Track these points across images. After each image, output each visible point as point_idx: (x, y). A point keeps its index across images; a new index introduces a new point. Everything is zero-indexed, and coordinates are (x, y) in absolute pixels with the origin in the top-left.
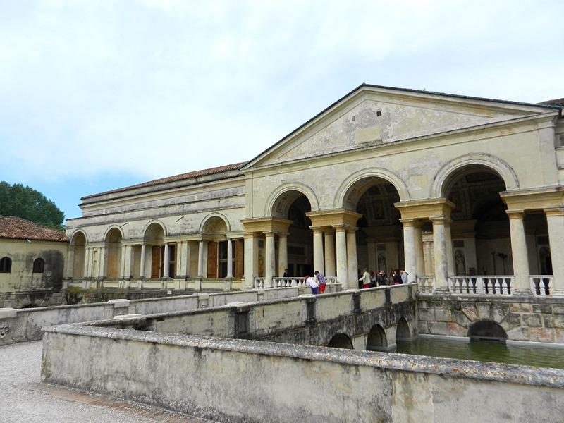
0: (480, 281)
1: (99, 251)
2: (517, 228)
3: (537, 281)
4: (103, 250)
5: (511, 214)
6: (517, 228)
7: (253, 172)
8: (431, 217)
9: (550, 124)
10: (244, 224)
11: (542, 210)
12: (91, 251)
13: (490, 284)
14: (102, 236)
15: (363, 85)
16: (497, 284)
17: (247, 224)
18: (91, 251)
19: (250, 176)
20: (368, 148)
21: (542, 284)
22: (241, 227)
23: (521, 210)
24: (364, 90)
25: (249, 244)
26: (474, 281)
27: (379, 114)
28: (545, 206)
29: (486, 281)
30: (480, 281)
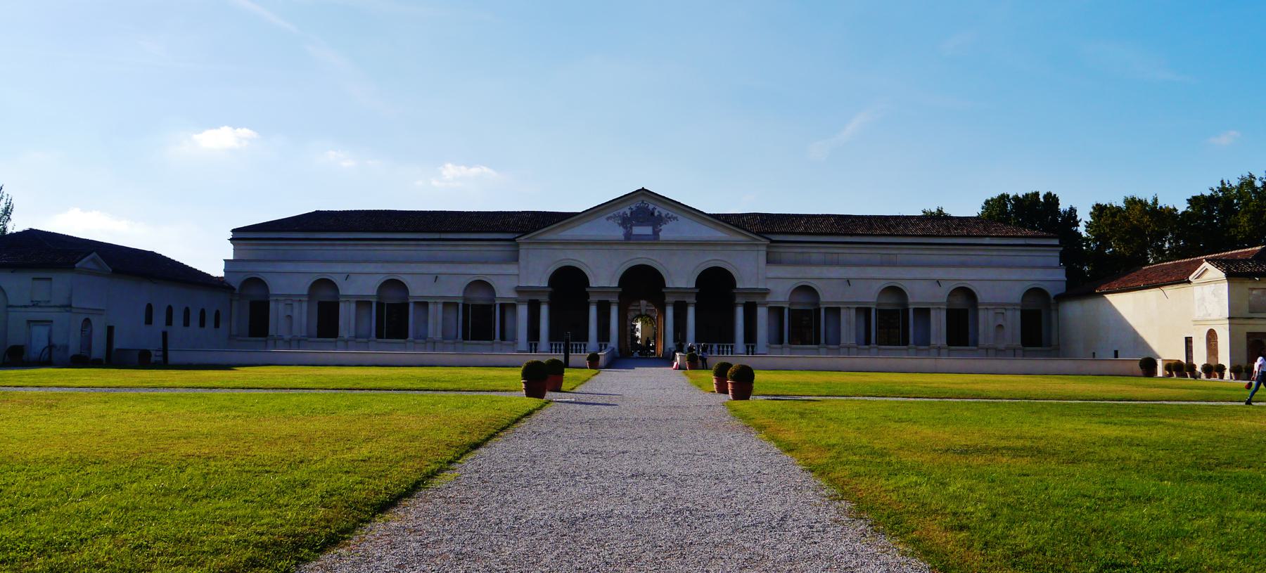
0: (715, 346)
1: (296, 305)
2: (740, 312)
3: (748, 347)
4: (305, 305)
6: (740, 312)
7: (529, 243)
8: (688, 300)
9: (764, 248)
11: (755, 302)
12: (281, 306)
13: (721, 349)
14: (302, 286)
16: (725, 349)
17: (520, 290)
18: (281, 306)
19: (525, 247)
20: (641, 241)
22: (513, 295)
23: (744, 302)
25: (523, 311)
26: (711, 347)
27: (652, 214)
28: (758, 300)
29: (719, 347)
30: (715, 346)
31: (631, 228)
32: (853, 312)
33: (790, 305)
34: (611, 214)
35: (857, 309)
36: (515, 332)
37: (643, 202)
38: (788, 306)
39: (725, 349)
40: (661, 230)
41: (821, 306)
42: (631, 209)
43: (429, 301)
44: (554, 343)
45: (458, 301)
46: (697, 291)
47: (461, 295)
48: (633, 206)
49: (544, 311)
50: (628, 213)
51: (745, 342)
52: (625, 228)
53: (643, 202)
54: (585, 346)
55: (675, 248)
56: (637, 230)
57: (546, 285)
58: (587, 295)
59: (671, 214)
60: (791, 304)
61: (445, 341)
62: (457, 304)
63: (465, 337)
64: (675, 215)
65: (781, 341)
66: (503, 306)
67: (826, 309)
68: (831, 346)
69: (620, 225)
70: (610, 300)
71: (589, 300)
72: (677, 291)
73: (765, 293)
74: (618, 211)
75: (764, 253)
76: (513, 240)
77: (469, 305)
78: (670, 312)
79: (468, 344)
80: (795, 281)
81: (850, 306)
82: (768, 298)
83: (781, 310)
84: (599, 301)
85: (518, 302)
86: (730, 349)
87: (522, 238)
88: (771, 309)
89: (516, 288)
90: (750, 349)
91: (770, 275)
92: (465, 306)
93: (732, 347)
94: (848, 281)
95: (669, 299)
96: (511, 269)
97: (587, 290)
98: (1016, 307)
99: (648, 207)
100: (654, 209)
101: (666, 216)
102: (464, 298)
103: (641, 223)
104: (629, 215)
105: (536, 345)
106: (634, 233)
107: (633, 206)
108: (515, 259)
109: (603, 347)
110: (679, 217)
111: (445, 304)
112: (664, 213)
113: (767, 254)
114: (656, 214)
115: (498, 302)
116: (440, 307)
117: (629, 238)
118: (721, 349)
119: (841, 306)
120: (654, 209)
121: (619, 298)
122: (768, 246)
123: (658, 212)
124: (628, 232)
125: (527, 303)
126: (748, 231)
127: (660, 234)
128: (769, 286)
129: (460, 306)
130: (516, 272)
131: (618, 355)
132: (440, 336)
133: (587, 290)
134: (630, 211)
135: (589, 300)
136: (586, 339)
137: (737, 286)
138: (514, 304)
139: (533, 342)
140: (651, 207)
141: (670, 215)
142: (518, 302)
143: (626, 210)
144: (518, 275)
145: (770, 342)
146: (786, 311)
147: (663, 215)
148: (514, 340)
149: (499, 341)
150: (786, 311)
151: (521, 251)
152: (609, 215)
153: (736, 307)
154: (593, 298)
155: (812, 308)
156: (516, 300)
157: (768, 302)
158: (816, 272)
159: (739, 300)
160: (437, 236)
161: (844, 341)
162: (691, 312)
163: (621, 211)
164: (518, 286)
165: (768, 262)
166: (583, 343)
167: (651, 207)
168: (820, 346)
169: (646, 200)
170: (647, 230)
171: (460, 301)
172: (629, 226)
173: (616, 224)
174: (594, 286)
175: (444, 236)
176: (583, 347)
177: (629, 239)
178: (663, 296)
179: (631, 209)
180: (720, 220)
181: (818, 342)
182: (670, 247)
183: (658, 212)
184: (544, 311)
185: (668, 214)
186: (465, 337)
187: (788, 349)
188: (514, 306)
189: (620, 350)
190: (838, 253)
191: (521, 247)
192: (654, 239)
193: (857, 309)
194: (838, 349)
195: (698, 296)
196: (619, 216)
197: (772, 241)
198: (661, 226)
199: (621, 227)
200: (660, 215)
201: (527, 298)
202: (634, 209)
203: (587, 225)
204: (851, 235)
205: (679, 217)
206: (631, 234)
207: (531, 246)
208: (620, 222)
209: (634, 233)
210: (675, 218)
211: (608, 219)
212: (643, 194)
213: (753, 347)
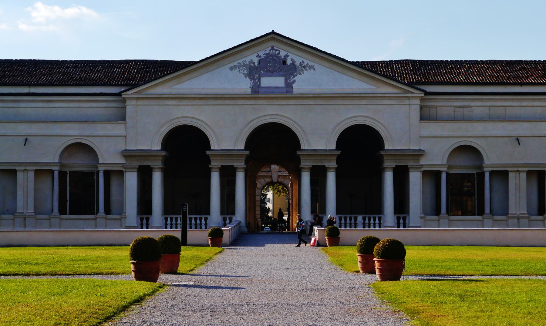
0: (360, 218)
2: (389, 178)
3: (398, 219)
5: (386, 168)
6: (389, 178)
7: (138, 98)
8: (327, 165)
9: (418, 102)
10: (124, 155)
13: (367, 221)
15: (273, 32)
16: (372, 221)
17: (128, 155)
19: (134, 102)
21: (401, 221)
22: (122, 161)
23: (394, 165)
24: (273, 37)
26: (356, 219)
27: (284, 62)
28: (410, 164)
29: (364, 219)
31: (259, 79)
32: (524, 176)
33: (448, 168)
34: (236, 63)
35: (529, 173)
36: (122, 204)
37: (273, 48)
38: (445, 169)
39: (372, 221)
40: (294, 81)
41: (485, 169)
42: (258, 56)
43: (17, 168)
44: (169, 217)
45: (53, 168)
46: (339, 153)
47: (57, 160)
48: (262, 54)
49: (157, 178)
50: (256, 61)
51: (395, 213)
52: (252, 79)
53: (273, 48)
54: (206, 219)
55: (311, 102)
56: (266, 82)
57: (159, 148)
58: (208, 160)
59: (306, 62)
60: (449, 167)
61: (38, 216)
62: (52, 172)
63: (62, 211)
64: (311, 64)
65: (437, 211)
66: (107, 174)
67: (492, 173)
68: (496, 217)
69: (246, 76)
70: (236, 164)
71: (210, 166)
72: (315, 153)
73: (418, 154)
74: (244, 59)
75: (418, 108)
76: (119, 94)
77: (65, 173)
78: (306, 178)
79: (67, 219)
80: (456, 140)
81: (520, 169)
82: (423, 161)
83: (438, 174)
84: (222, 166)
86: (377, 221)
87: (130, 92)
88: (425, 173)
89: (123, 152)
90: (401, 221)
91: (425, 133)
92: (62, 174)
93: (380, 219)
94: (517, 139)
95: (306, 163)
96: (118, 129)
97: (208, 153)
99: (279, 54)
100: (287, 56)
101: (301, 64)
102: (61, 165)
103: (271, 74)
104: (256, 64)
105: (148, 219)
106: (262, 85)
107: (262, 54)
108: (122, 118)
109: (228, 221)
110: (316, 66)
111: (38, 173)
113: (421, 108)
114: (289, 62)
115: (101, 169)
116: (31, 175)
117: (256, 90)
118: (367, 221)
119: (509, 169)
120: (287, 56)
121: (246, 162)
122: (422, 99)
123: (292, 60)
124: (255, 84)
125: (136, 170)
126: (398, 81)
127: (294, 85)
128: (423, 146)
129: (56, 174)
131: (245, 229)
132: (31, 210)
133: (208, 153)
134: (258, 58)
135: (210, 166)
136: (207, 211)
137: (387, 147)
138: (122, 170)
139: (145, 216)
140: (282, 54)
141: (305, 64)
142: (126, 168)
143: (253, 57)
145: (425, 212)
146: (444, 176)
147: (297, 64)
148: (121, 213)
149: (104, 215)
150: (444, 176)
151: (128, 107)
152: (232, 65)
153: (384, 172)
154: (215, 163)
155: (474, 172)
156: (123, 167)
157: (422, 165)
158: (478, 129)
159: (389, 163)
160: (26, 90)
161: (512, 210)
162: (331, 178)
163: (248, 59)
164: (126, 150)
165: (422, 118)
166: (203, 216)
167: (282, 54)
168: (485, 216)
169: (277, 45)
170: (278, 82)
171: (56, 168)
172: (256, 76)
173: (242, 74)
174: (216, 148)
175: (34, 90)
176: (203, 222)
177: (258, 93)
178: (297, 160)
179: (258, 56)
180: (365, 69)
181: (481, 212)
182: (305, 102)
183: (292, 60)
184: (157, 178)
185: (303, 62)
186: (62, 211)
187: (446, 221)
188: (120, 174)
189: (248, 224)
190: (506, 106)
191: (128, 103)
192: (287, 92)
193: (529, 173)
194: (507, 220)
195: (339, 160)
196: (245, 65)
197: (427, 93)
198: (294, 76)
199: (247, 78)
200: (293, 64)
201: (137, 164)
202: (263, 57)
204: (522, 84)
205: (316, 66)
206: (259, 86)
207: (140, 102)
208: (246, 72)
209: (262, 85)
211: (231, 69)
212: (273, 38)
213: (404, 219)
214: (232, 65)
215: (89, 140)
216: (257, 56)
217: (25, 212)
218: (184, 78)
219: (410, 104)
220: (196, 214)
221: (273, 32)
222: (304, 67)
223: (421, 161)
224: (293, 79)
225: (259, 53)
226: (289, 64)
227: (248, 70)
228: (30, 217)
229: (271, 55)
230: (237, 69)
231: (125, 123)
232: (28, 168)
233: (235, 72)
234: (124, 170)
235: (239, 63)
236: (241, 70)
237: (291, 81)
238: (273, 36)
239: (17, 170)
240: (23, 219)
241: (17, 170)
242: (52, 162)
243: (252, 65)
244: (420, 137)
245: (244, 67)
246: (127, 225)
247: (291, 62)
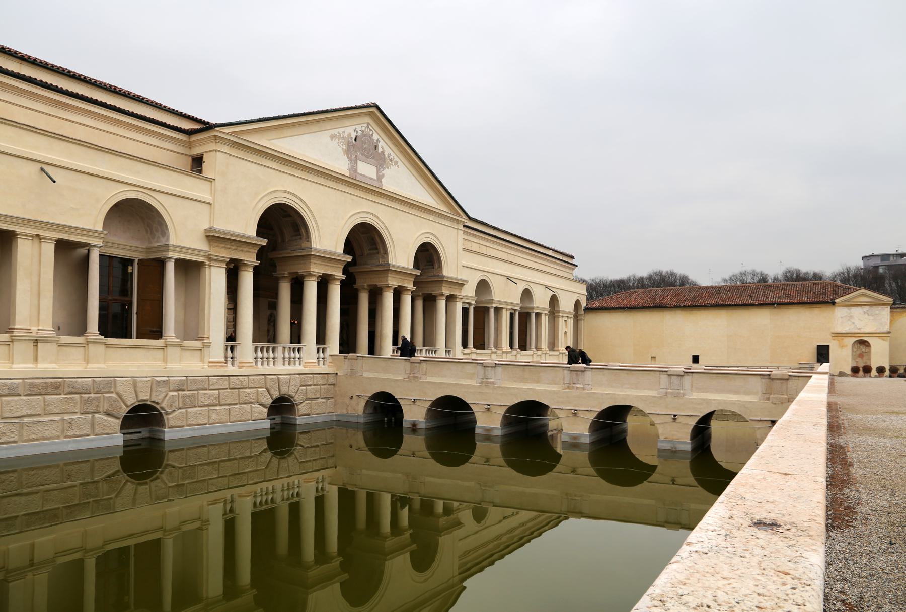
17: (214, 238)
27: (376, 147)
43: (18, 229)
64: (396, 159)
85: (210, 260)
98: (569, 316)
107: (359, 128)
110: (400, 163)
112: (387, 151)
114: (380, 150)
130: (208, 197)
141: (391, 157)
142: (210, 260)
144: (210, 204)
147: (386, 154)
167: (376, 137)
170: (367, 170)
196: (344, 138)
200: (383, 152)
203: (306, 137)
210: (396, 163)
211: (333, 137)
214: (335, 132)
215: (154, 196)
216: (354, 130)
217: (34, 329)
218: (288, 132)
219: (458, 229)
220: (269, 342)
221: (377, 107)
222: (391, 160)
223: (462, 292)
224: (382, 172)
225: (357, 126)
226: (380, 152)
227: (347, 146)
228: (47, 341)
229: (366, 135)
230: (337, 141)
231: (212, 181)
232: (42, 233)
233: (335, 143)
234: (207, 262)
235: (339, 133)
236: (341, 142)
237: (381, 174)
238: (374, 111)
239: (17, 235)
240: (32, 344)
241: (17, 235)
242: (91, 228)
243: (350, 139)
244: (463, 266)
245: (343, 141)
246: (211, 360)
247: (382, 150)
